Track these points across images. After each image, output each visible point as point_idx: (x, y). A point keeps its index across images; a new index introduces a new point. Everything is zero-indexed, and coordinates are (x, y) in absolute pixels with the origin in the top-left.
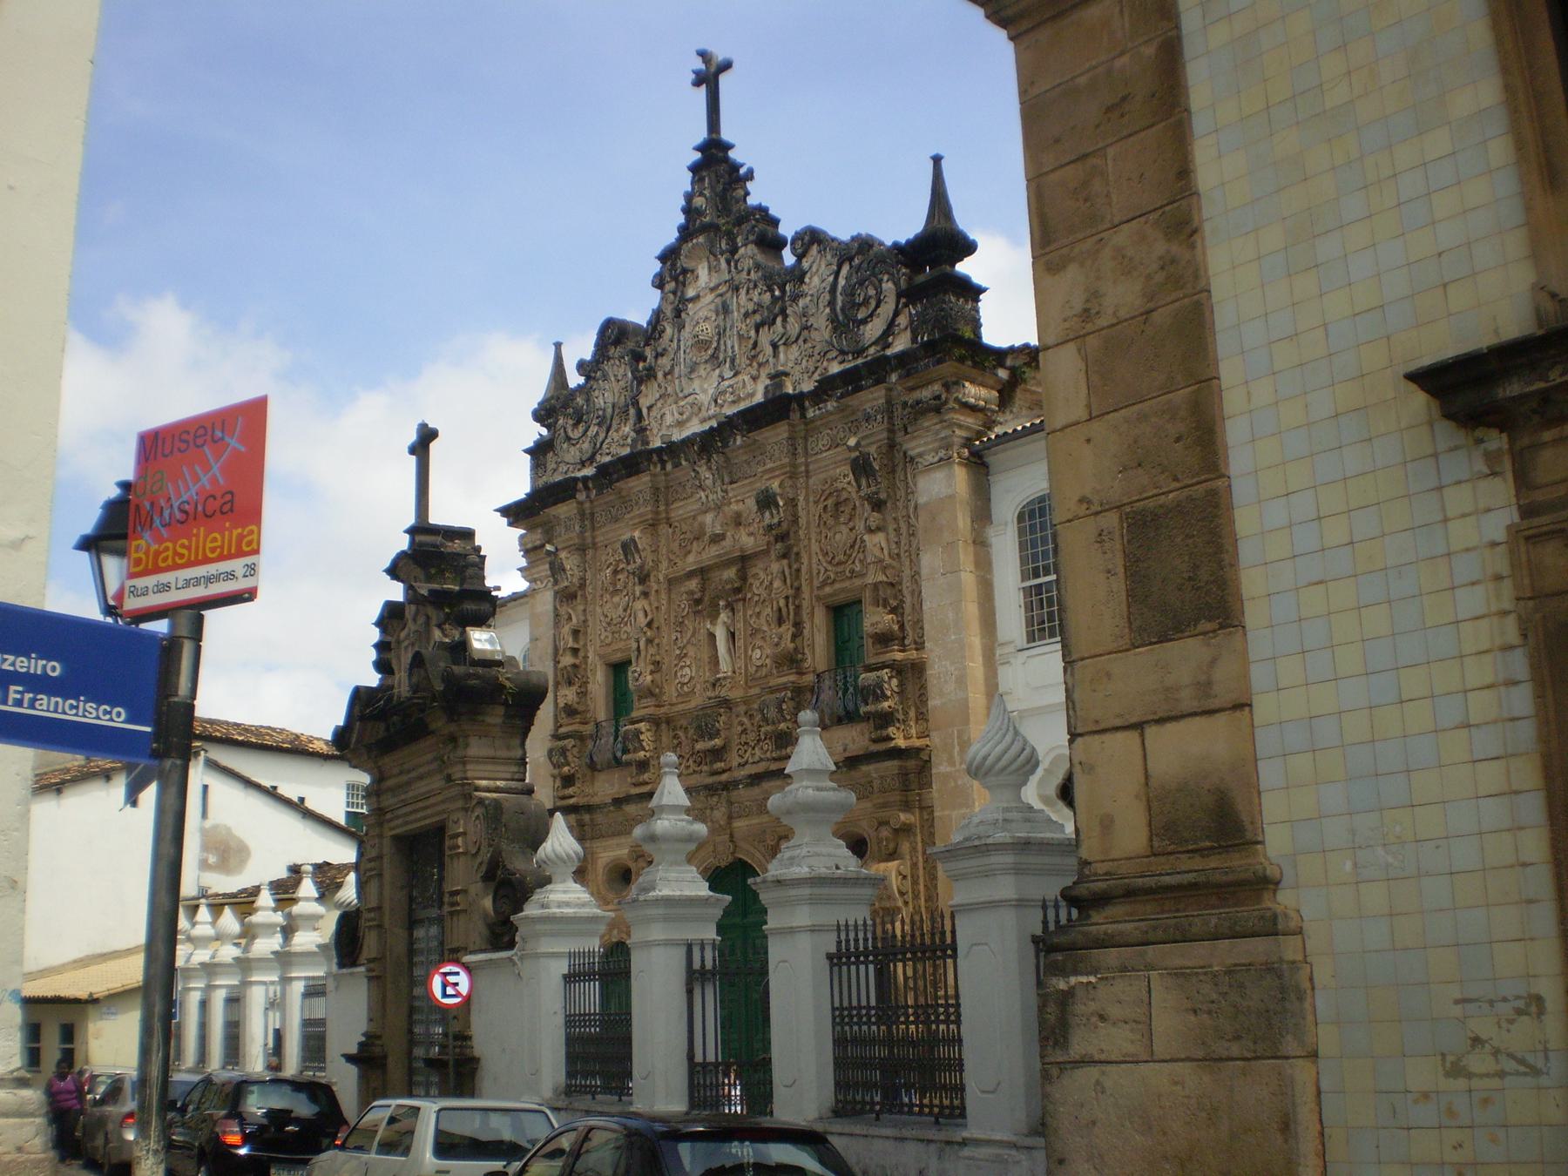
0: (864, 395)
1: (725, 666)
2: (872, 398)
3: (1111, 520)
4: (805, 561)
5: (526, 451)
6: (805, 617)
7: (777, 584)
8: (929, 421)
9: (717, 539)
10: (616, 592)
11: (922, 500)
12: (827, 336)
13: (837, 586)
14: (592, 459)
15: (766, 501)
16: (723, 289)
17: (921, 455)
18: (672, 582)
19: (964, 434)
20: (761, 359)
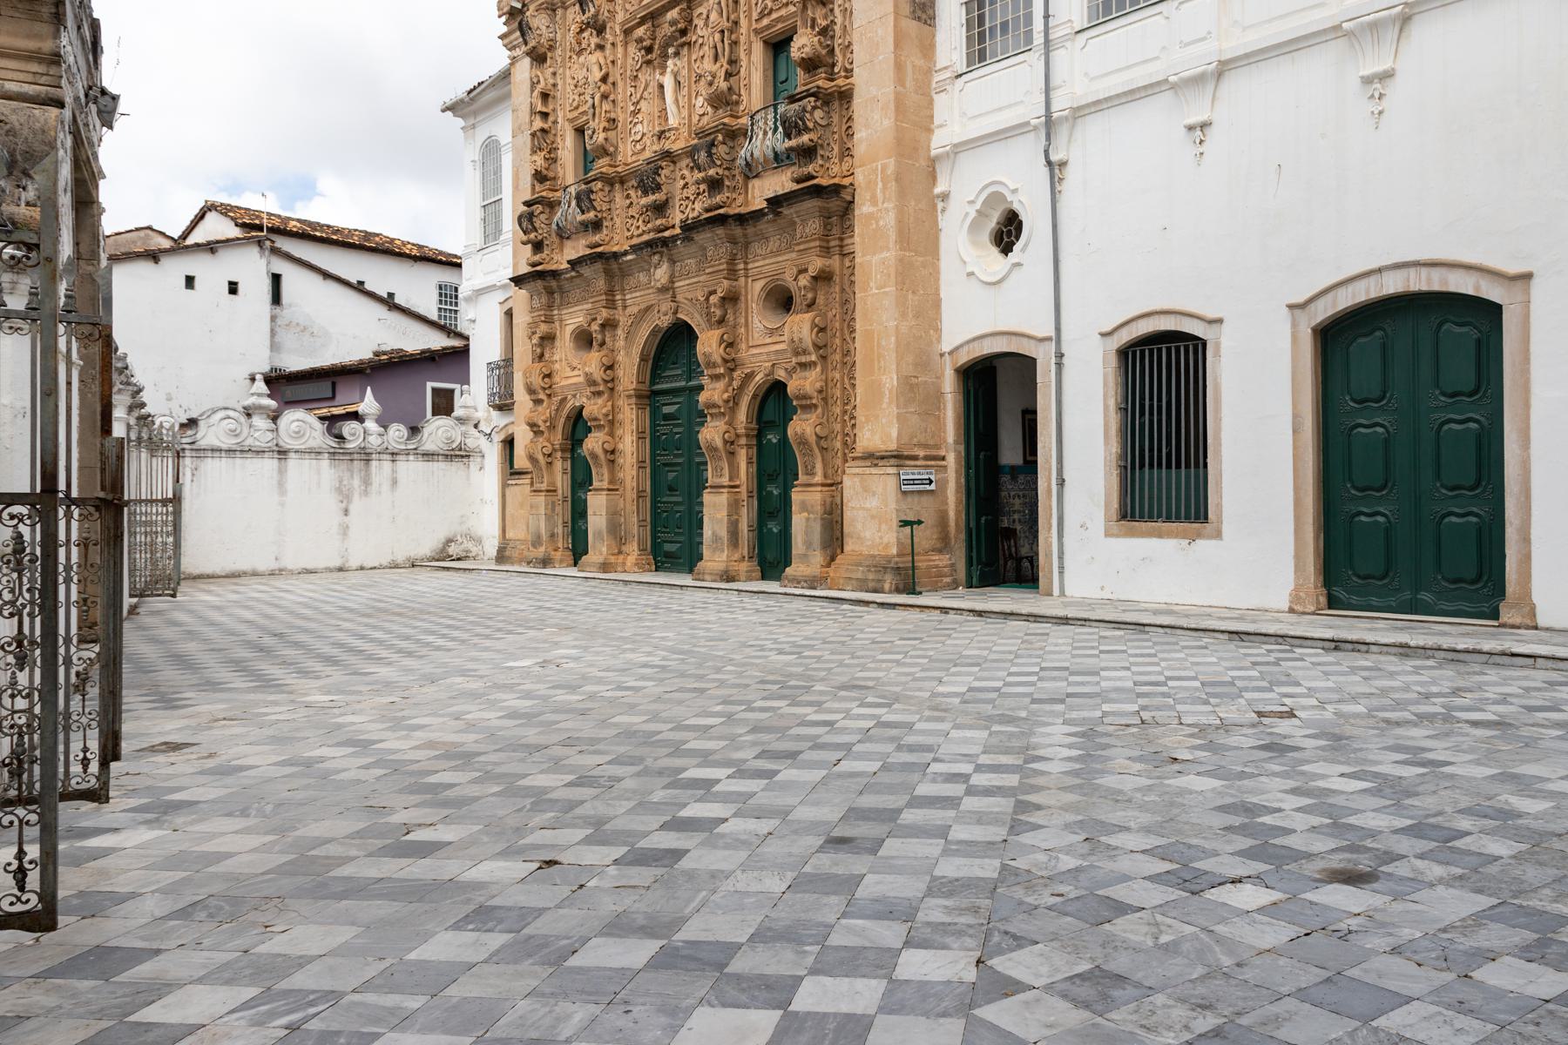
1: (673, 121)
6: (743, 55)
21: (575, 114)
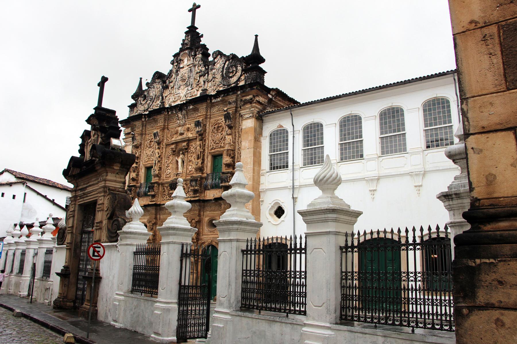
0: (229, 97)
1: (180, 170)
2: (232, 98)
3: (494, 29)
4: (207, 142)
5: (129, 106)
6: (205, 158)
7: (198, 148)
8: (248, 106)
9: (182, 134)
10: (150, 147)
11: (243, 127)
12: (220, 80)
13: (216, 150)
14: (147, 110)
15: (198, 124)
16: (191, 66)
17: (244, 115)
18: (167, 145)
19: (258, 110)
20: (200, 85)
21: (147, 163)
